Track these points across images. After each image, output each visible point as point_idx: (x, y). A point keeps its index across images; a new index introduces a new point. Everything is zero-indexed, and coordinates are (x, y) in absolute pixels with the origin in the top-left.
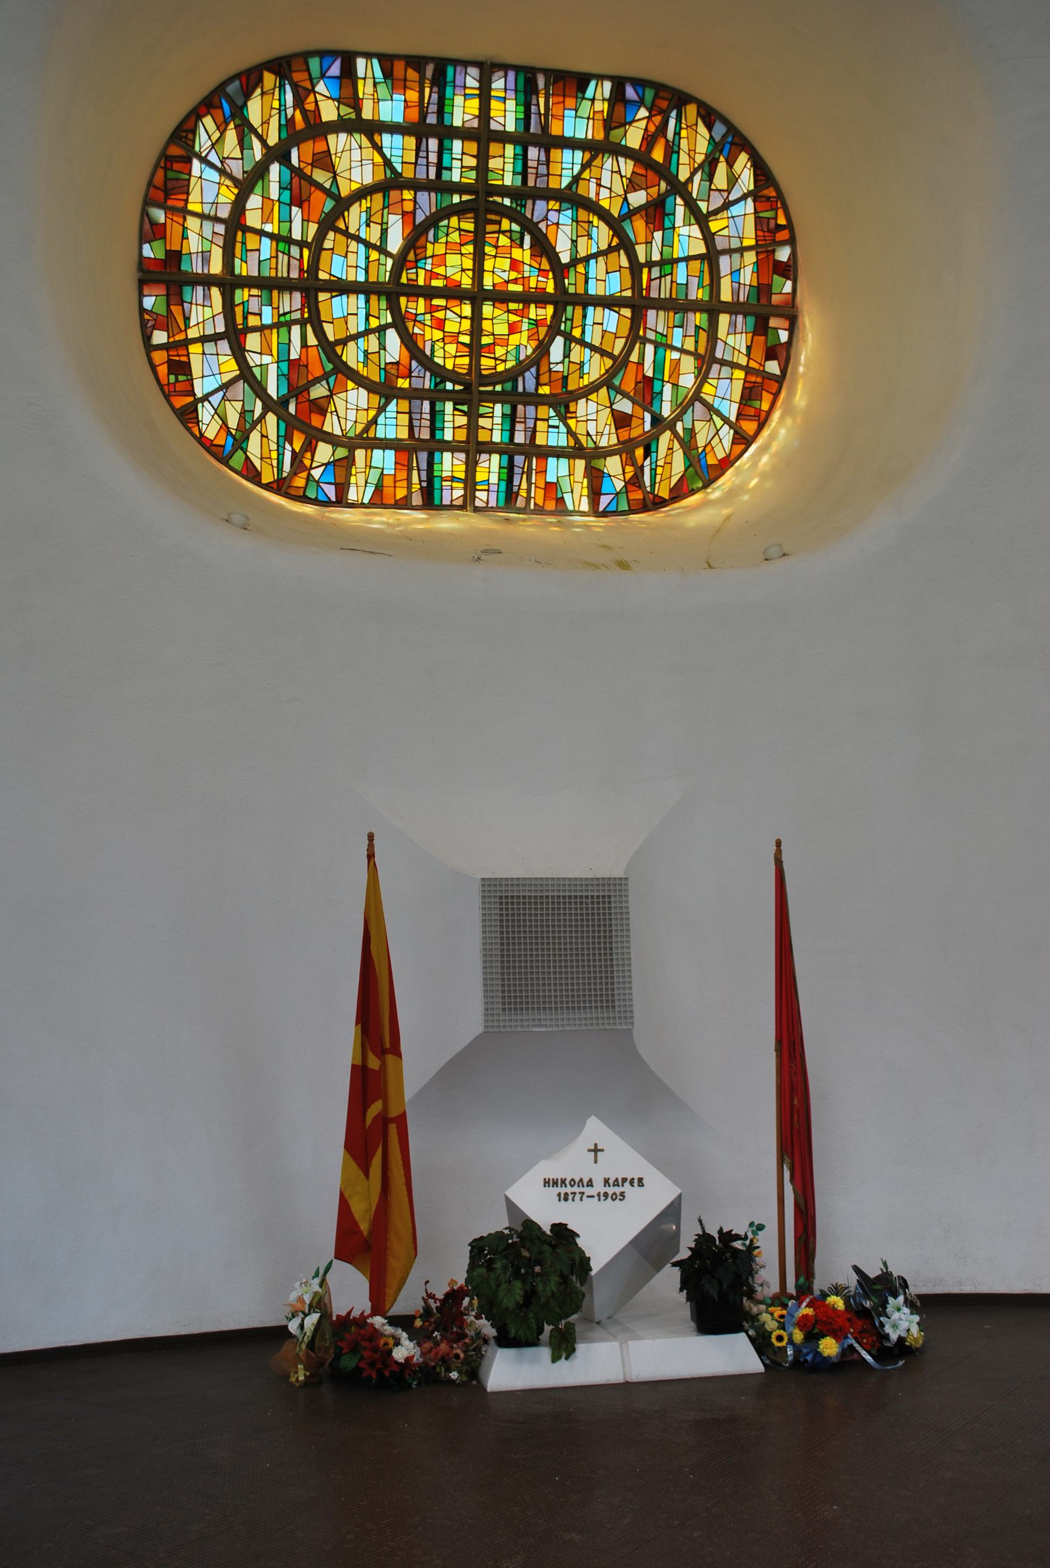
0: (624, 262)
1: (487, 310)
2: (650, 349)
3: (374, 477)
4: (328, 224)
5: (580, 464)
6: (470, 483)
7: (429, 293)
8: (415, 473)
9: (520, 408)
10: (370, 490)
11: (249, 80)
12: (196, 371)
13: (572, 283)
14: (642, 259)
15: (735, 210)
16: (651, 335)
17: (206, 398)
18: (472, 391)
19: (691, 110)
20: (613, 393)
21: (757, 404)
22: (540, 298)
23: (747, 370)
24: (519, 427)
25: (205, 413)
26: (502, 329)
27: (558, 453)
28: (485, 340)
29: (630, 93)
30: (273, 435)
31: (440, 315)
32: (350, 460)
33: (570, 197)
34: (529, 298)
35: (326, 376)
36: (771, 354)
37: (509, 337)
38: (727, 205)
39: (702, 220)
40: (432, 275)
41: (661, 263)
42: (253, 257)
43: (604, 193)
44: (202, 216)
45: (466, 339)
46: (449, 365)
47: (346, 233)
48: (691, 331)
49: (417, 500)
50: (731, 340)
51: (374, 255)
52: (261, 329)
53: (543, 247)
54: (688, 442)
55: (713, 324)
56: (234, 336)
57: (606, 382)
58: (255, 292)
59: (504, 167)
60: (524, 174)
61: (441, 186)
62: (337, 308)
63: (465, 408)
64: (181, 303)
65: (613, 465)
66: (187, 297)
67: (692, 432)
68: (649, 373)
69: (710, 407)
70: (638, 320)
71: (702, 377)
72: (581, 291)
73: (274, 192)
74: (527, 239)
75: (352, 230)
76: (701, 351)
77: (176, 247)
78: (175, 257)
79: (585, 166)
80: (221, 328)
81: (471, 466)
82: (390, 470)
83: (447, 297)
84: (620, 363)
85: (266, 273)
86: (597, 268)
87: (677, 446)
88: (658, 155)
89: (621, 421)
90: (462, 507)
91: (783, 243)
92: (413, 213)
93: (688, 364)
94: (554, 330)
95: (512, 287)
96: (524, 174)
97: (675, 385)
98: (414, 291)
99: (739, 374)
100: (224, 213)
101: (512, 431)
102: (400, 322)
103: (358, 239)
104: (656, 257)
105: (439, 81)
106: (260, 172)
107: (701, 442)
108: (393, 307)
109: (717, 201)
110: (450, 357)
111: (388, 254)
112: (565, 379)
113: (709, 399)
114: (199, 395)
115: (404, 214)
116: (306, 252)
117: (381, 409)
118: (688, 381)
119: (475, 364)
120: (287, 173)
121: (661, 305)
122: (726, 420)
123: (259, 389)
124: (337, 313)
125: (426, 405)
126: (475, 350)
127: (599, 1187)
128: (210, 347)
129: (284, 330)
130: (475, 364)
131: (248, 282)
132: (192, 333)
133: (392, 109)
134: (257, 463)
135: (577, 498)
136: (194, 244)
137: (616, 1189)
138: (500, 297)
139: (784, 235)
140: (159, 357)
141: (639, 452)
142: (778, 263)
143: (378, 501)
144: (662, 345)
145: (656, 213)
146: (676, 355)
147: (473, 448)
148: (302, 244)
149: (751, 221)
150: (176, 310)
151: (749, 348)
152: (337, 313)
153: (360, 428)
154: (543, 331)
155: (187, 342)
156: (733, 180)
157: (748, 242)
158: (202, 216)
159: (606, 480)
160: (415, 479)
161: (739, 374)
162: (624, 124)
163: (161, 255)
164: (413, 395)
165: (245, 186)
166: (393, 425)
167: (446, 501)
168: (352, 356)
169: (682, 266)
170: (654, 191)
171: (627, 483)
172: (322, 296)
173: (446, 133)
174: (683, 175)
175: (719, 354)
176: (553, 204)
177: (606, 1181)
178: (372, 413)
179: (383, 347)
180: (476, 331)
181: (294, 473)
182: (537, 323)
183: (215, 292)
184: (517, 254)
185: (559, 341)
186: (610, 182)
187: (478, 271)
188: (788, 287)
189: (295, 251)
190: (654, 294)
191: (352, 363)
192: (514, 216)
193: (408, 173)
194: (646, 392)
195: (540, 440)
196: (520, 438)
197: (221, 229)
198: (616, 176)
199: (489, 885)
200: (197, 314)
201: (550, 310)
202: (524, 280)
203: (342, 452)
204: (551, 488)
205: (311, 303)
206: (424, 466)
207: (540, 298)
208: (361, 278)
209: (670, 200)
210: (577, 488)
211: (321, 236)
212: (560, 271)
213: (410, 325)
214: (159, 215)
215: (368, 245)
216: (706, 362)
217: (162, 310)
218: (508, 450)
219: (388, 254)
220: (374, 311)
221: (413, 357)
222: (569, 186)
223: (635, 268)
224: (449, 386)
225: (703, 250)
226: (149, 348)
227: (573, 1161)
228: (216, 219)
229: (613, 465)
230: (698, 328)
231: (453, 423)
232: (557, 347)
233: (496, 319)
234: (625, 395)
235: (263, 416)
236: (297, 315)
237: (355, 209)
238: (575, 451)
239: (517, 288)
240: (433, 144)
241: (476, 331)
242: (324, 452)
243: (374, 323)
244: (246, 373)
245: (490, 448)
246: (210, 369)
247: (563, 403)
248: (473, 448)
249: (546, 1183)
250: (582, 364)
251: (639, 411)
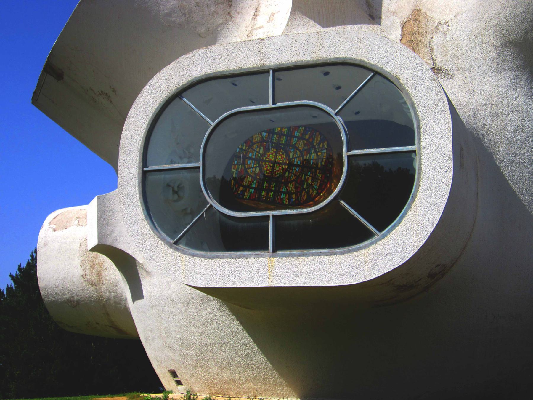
3: (249, 194)
7: (266, 161)
19: (318, 133)
23: (320, 180)
27: (284, 193)
29: (308, 129)
33: (295, 147)
38: (322, 150)
39: (316, 152)
40: (266, 158)
53: (288, 155)
54: (308, 193)
55: (316, 172)
65: (294, 196)
67: (309, 191)
71: (312, 181)
79: (297, 141)
82: (253, 192)
88: (311, 140)
89: (296, 188)
93: (310, 178)
97: (307, 182)
98: (263, 161)
99: (319, 181)
103: (254, 150)
107: (311, 193)
109: (320, 149)
118: (310, 181)
122: (316, 189)
124: (249, 163)
138: (278, 163)
143: (249, 199)
145: (309, 151)
147: (268, 191)
148: (244, 150)
152: (249, 163)
156: (323, 146)
161: (319, 181)
162: (306, 134)
168: (250, 171)
174: (315, 144)
179: (256, 170)
182: (284, 169)
186: (301, 145)
196: (277, 189)
202: (283, 161)
215: (256, 152)
216: (314, 178)
225: (315, 158)
229: (294, 196)
232: (287, 174)
237: (255, 145)
240: (271, 135)
248: (268, 191)
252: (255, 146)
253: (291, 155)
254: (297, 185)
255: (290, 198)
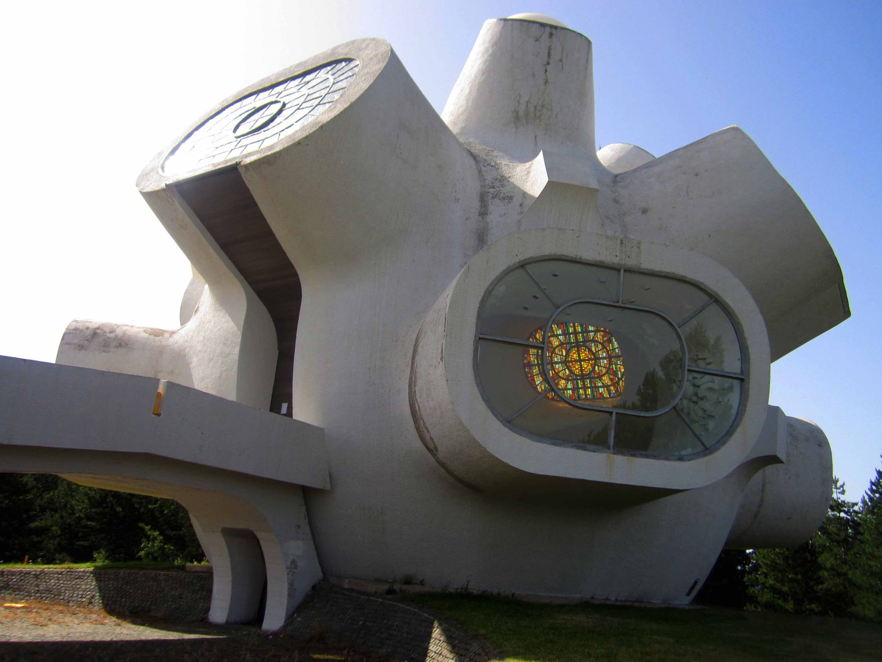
4: (552, 353)
7: (572, 362)
11: (536, 332)
18: (583, 377)
33: (593, 341)
34: (590, 359)
53: (590, 350)
59: (580, 337)
61: (570, 343)
65: (612, 388)
78: (530, 362)
81: (585, 391)
84: (609, 368)
89: (611, 380)
94: (595, 365)
98: (569, 362)
105: (566, 326)
110: (577, 372)
121: (614, 357)
126: (582, 370)
133: (560, 332)
135: (606, 395)
144: (616, 364)
145: (609, 341)
147: (585, 388)
166: (569, 386)
168: (561, 374)
173: (569, 334)
180: (581, 367)
186: (599, 337)
192: (583, 346)
194: (615, 373)
204: (601, 394)
212: (594, 354)
218: (591, 387)
223: (608, 351)
226: (527, 377)
229: (612, 388)
232: (596, 368)
233: (585, 365)
241: (581, 367)
246: (538, 380)
247: (600, 377)
248: (585, 388)
252: (557, 350)
253: (593, 349)
255: (609, 391)
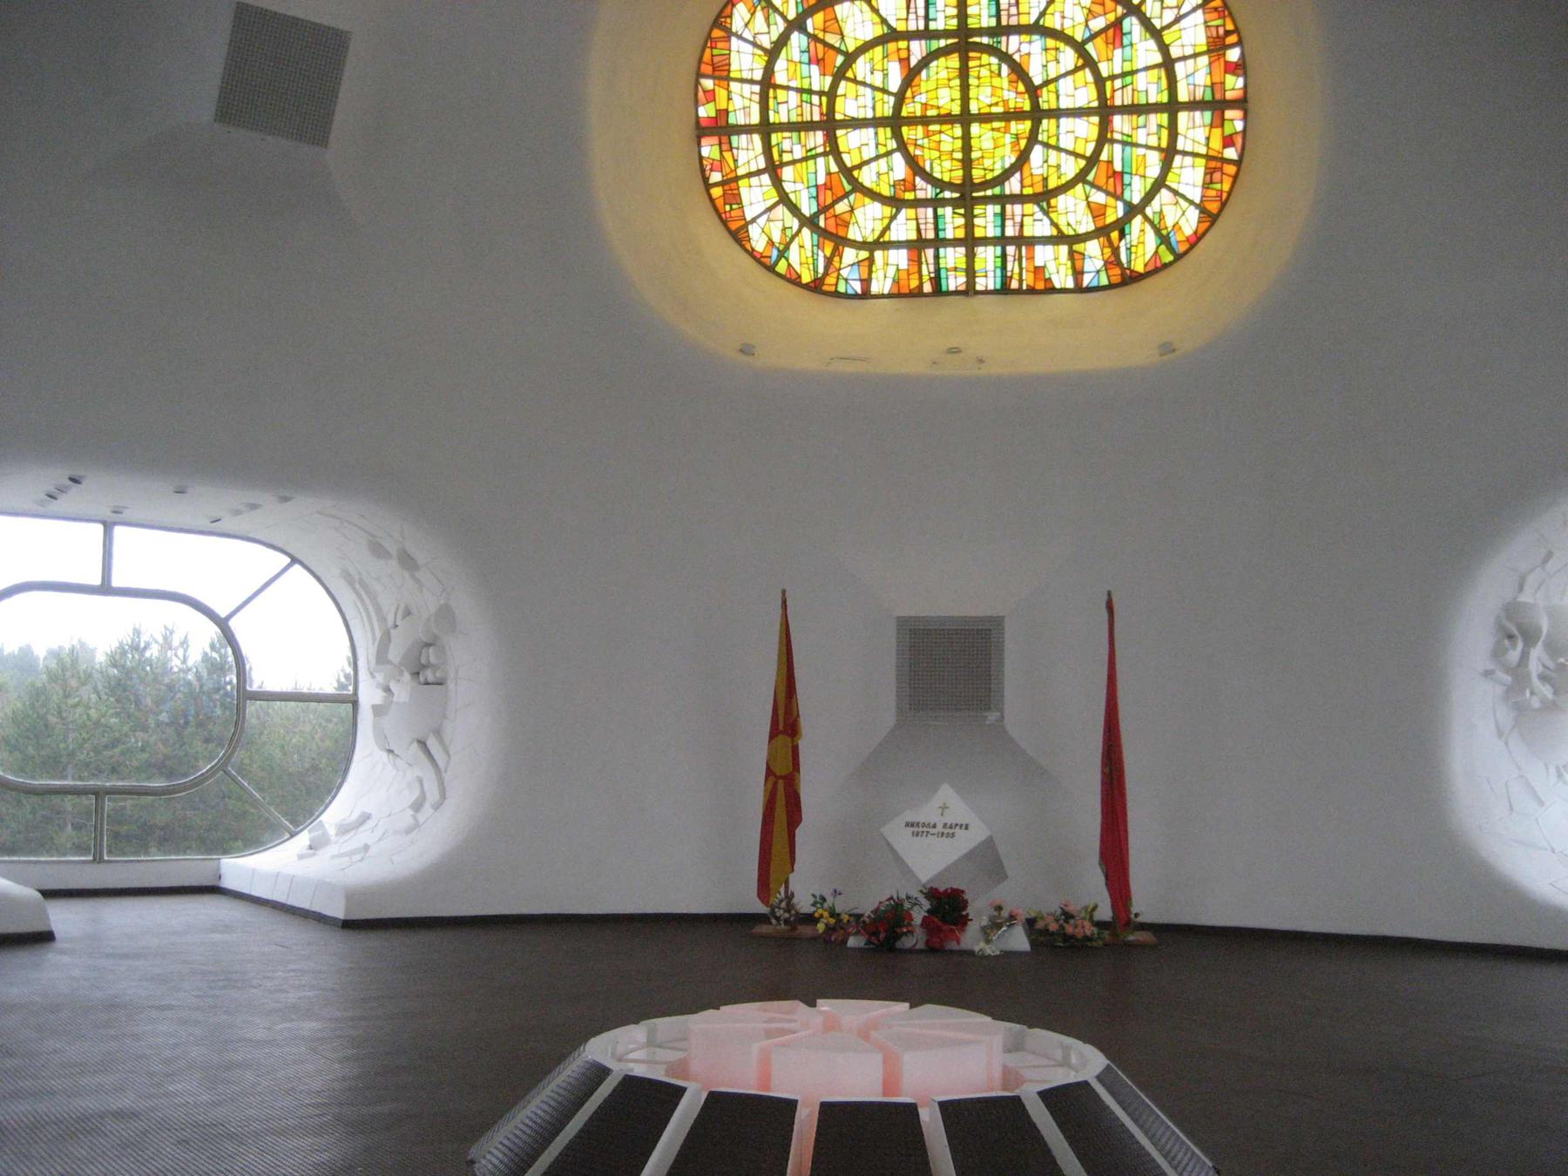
0: (1090, 78)
1: (975, 128)
2: (1117, 148)
3: (891, 272)
4: (839, 75)
5: (1064, 249)
6: (971, 272)
7: (924, 121)
8: (924, 267)
9: (1008, 207)
10: (889, 282)
12: (745, 201)
13: (1047, 100)
14: (1105, 74)
15: (1184, 23)
16: (1117, 136)
17: (754, 220)
18: (967, 195)
20: (1088, 188)
21: (1218, 186)
22: (1018, 115)
23: (1208, 157)
24: (1009, 223)
25: (754, 231)
26: (987, 143)
28: (974, 155)
30: (808, 245)
31: (936, 138)
32: (871, 260)
35: (846, 195)
36: (1228, 141)
37: (994, 149)
38: (1178, 20)
39: (1156, 34)
40: (925, 106)
41: (1124, 75)
42: (783, 108)
43: (1068, 24)
44: (742, 81)
45: (959, 155)
46: (946, 179)
47: (855, 81)
48: (1154, 129)
49: (927, 288)
50: (1190, 134)
51: (879, 95)
52: (793, 162)
53: (1019, 72)
56: (773, 169)
57: (1081, 177)
58: (787, 134)
60: (998, 16)
62: (849, 141)
63: (962, 211)
64: (731, 149)
66: (735, 144)
68: (1118, 167)
69: (1176, 193)
70: (1105, 126)
71: (1167, 166)
72: (1053, 106)
73: (796, 57)
74: (1005, 68)
75: (859, 78)
76: (1164, 144)
77: (723, 106)
80: (762, 164)
81: (970, 257)
82: (904, 265)
83: (941, 123)
84: (1093, 160)
85: (794, 119)
86: (1065, 85)
87: (1148, 227)
89: (1097, 211)
90: (965, 293)
91: (1232, 46)
92: (908, 59)
95: (995, 110)
96: (998, 16)
98: (912, 121)
100: (758, 76)
101: (1003, 226)
102: (902, 147)
103: (864, 84)
104: (1117, 71)
106: (782, 41)
107: (1169, 222)
108: (897, 135)
109: (1169, 16)
111: (889, 93)
112: (1045, 180)
113: (1174, 186)
114: (748, 218)
115: (901, 60)
116: (824, 99)
117: (893, 218)
119: (968, 176)
120: (804, 39)
123: (794, 210)
125: (930, 211)
126: (967, 163)
127: (939, 828)
128: (754, 180)
129: (811, 162)
130: (968, 176)
131: (782, 127)
132: (741, 172)
134: (797, 268)
135: (1063, 279)
136: (737, 103)
137: (949, 831)
138: (985, 118)
139: (1233, 39)
140: (717, 192)
141: (1115, 235)
142: (1227, 63)
145: (1115, 32)
146: (1141, 151)
147: (970, 242)
148: (821, 93)
149: (1202, 29)
150: (727, 155)
151: (1208, 139)
153: (877, 234)
154: (1023, 143)
155: (737, 178)
157: (1198, 50)
158: (742, 81)
159: (1087, 261)
160: (925, 271)
161: (1202, 162)
163: (713, 114)
164: (917, 203)
165: (773, 54)
166: (903, 229)
167: (952, 288)
168: (866, 177)
169: (1141, 77)
170: (1111, 17)
171: (1107, 263)
172: (839, 133)
175: (1180, 146)
176: (1025, 38)
177: (945, 825)
178: (886, 222)
180: (967, 148)
181: (826, 274)
183: (756, 138)
184: (996, 81)
185: (1037, 151)
187: (965, 99)
188: (1240, 82)
189: (815, 99)
190: (1118, 102)
191: (867, 184)
193: (901, 27)
195: (1027, 233)
197: (757, 88)
198: (1078, 8)
199: (903, 622)
200: (743, 157)
201: (1028, 124)
203: (864, 254)
204: (1039, 271)
205: (831, 140)
206: (931, 260)
207: (1018, 115)
208: (870, 115)
209: (1126, 24)
210: (1062, 268)
211: (834, 86)
212: (1033, 91)
213: (911, 149)
214: (708, 84)
215: (874, 88)
216: (1169, 154)
217: (716, 154)
219: (889, 93)
220: (881, 139)
221: (915, 174)
222: (1037, 21)
223: (1100, 82)
224: (947, 194)
226: (708, 186)
227: (928, 813)
228: (752, 82)
230: (1160, 126)
231: (953, 224)
232: (1037, 153)
234: (1099, 188)
235: (799, 231)
236: (820, 150)
238: (1059, 238)
239: (1000, 109)
241: (967, 148)
242: (850, 255)
243: (882, 150)
244: (784, 199)
245: (985, 241)
246: (756, 196)
247: (1044, 197)
248: (970, 242)
249: (907, 825)
250: (1058, 167)
251: (1111, 201)
252: (861, 68)
254: (1098, 197)
